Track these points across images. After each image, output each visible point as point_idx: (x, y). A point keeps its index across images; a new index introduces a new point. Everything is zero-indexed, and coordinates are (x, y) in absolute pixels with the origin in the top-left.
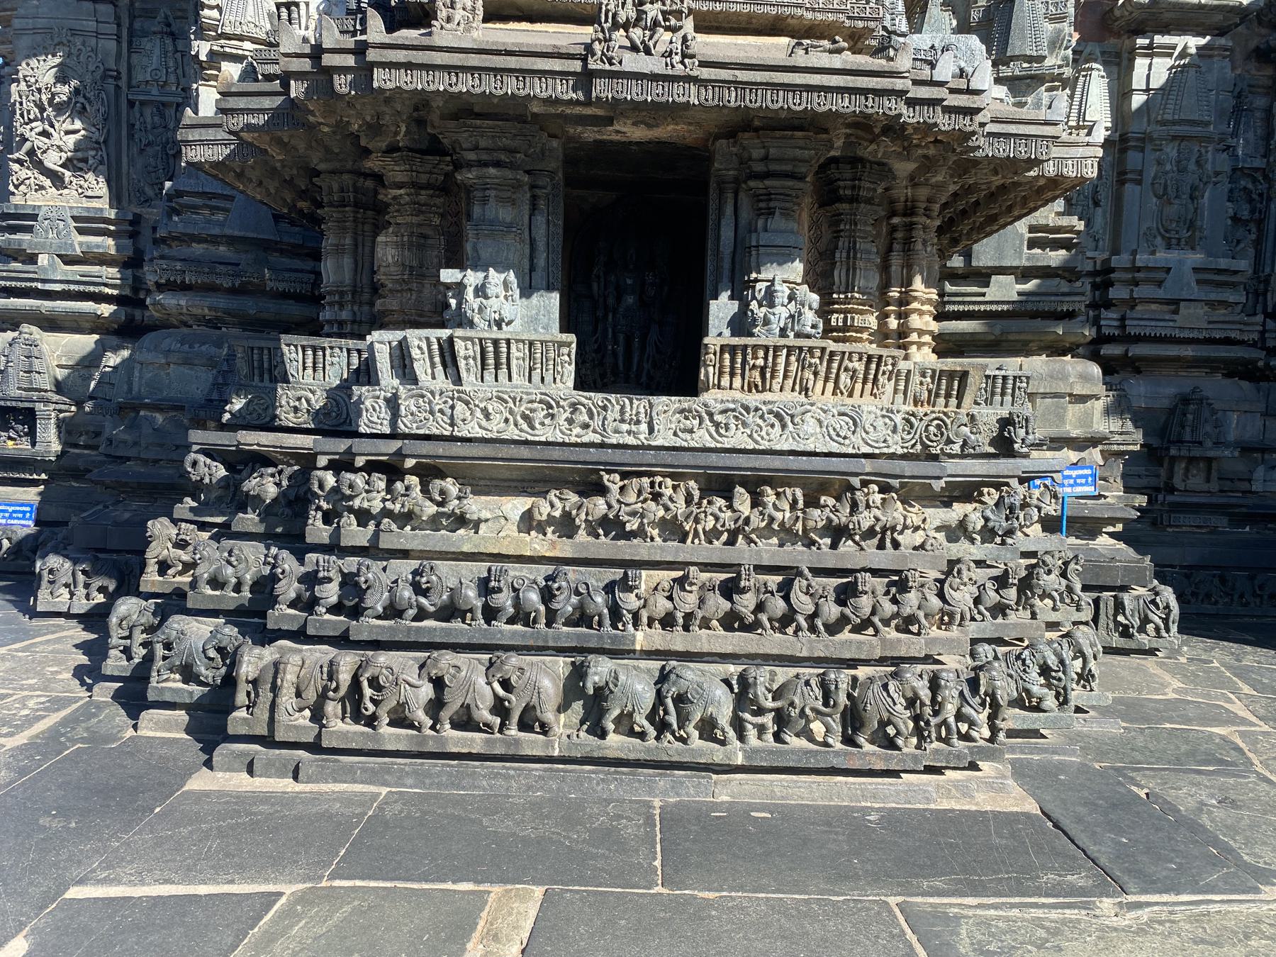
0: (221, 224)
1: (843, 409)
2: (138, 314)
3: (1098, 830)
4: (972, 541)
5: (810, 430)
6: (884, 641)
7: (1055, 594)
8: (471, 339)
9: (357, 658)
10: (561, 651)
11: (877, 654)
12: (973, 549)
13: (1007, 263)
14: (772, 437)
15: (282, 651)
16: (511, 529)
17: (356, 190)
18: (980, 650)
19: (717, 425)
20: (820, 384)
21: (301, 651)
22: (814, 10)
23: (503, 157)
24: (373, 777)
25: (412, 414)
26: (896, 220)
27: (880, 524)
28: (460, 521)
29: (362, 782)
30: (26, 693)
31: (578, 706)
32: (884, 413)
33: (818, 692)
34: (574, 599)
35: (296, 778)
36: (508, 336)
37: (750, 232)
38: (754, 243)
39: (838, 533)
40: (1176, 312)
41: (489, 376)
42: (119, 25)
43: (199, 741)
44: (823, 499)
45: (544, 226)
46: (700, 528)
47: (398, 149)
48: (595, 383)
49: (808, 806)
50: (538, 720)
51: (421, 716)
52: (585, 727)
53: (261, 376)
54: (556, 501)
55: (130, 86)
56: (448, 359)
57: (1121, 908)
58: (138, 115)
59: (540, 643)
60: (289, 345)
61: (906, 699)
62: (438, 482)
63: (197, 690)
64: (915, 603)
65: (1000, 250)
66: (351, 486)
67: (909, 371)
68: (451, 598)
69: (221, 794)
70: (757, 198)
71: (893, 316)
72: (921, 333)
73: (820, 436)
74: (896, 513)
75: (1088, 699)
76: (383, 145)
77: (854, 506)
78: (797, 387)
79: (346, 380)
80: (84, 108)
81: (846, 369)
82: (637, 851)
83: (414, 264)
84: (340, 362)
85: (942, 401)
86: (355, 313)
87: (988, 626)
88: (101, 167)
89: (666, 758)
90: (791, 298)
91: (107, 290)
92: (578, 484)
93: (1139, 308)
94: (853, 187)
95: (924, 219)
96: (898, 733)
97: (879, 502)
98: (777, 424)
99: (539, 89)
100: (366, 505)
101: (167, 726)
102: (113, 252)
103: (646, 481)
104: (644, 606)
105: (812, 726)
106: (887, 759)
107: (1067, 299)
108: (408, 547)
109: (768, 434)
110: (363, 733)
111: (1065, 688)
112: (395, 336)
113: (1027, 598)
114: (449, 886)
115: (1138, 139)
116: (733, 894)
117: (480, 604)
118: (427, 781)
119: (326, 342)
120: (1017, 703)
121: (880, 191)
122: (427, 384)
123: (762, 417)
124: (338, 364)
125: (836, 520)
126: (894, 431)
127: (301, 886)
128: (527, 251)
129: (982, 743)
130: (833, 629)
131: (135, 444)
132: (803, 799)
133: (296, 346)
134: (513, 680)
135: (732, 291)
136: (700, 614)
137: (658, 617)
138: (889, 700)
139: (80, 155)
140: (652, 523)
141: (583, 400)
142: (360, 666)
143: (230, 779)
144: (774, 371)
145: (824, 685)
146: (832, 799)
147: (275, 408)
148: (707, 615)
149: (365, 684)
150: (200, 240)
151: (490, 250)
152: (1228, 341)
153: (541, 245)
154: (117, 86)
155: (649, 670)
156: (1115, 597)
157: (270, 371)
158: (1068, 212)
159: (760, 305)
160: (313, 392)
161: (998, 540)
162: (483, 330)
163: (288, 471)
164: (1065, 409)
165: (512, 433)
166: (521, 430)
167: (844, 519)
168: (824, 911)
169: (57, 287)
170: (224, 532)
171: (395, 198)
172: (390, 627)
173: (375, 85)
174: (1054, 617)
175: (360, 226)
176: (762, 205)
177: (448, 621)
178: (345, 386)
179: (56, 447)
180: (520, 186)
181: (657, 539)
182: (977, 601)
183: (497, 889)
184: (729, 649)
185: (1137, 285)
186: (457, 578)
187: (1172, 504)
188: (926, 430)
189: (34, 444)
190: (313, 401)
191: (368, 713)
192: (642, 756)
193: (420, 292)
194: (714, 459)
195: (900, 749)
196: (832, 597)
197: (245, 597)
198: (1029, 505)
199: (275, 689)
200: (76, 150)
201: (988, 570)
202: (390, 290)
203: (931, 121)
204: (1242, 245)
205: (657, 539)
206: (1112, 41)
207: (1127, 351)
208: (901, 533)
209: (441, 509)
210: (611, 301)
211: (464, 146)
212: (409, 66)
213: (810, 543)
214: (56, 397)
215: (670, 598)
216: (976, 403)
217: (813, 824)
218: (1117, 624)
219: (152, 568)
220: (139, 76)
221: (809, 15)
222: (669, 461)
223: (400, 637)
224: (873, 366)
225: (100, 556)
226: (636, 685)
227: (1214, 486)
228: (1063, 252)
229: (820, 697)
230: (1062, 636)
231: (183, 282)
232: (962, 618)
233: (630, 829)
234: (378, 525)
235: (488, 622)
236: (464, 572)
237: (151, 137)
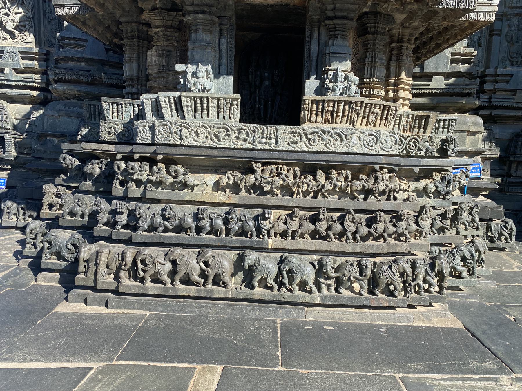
0: (82, 53)
1: (371, 132)
2: (49, 96)
3: (494, 338)
4: (429, 197)
5: (355, 142)
6: (389, 245)
7: (466, 223)
8: (189, 97)
9: (136, 250)
10: (232, 248)
11: (386, 251)
12: (430, 201)
13: (440, 70)
14: (336, 145)
15: (101, 246)
16: (209, 190)
18: (433, 249)
21: (109, 246)
23: (206, 9)
24: (143, 307)
25: (161, 134)
26: (393, 45)
27: (388, 188)
28: (185, 185)
29: (138, 309)
31: (241, 274)
32: (391, 134)
34: (239, 224)
35: (107, 306)
36: (208, 95)
37: (326, 46)
38: (327, 52)
39: (367, 193)
40: (515, 95)
41: (198, 115)
43: (64, 287)
44: (361, 176)
45: (226, 44)
46: (300, 190)
47: (157, 9)
49: (351, 323)
50: (221, 280)
51: (166, 278)
52: (244, 284)
53: (95, 118)
56: (179, 107)
57: (513, 381)
58: (47, 6)
59: (223, 244)
60: (105, 102)
63: (64, 264)
64: (404, 226)
65: (437, 64)
66: (132, 169)
68: (180, 222)
69: (70, 314)
70: (329, 30)
71: (391, 91)
72: (404, 99)
73: (360, 145)
74: (396, 183)
75: (481, 271)
76: (150, 7)
77: (376, 179)
78: (349, 121)
79: (132, 119)
81: (373, 113)
82: (269, 346)
83: (165, 64)
84: (128, 111)
85: (416, 130)
86: (138, 90)
87: (438, 238)
88: (31, 29)
90: (346, 78)
91: (35, 85)
93: (497, 93)
94: (375, 27)
95: (407, 44)
96: (396, 289)
97: (388, 178)
98: (339, 139)
100: (139, 177)
101: (50, 280)
102: (37, 67)
103: (274, 167)
104: (273, 227)
105: (353, 285)
106: (390, 301)
107: (468, 87)
108: (160, 198)
109: (334, 144)
110: (138, 286)
111: (473, 268)
112: (153, 96)
113: (455, 225)
114: (176, 365)
116: (317, 371)
117: (194, 225)
119: (122, 101)
120: (451, 275)
123: (331, 136)
124: (128, 111)
125: (367, 187)
126: (396, 143)
127: (102, 364)
128: (218, 56)
129: (435, 294)
130: (364, 239)
131: (45, 152)
133: (108, 103)
135: (317, 76)
136: (300, 231)
137: (279, 232)
138: (392, 273)
139: (22, 24)
140: (277, 187)
141: (244, 127)
142: (137, 254)
143: (76, 306)
145: (360, 266)
146: (362, 320)
147: (100, 132)
148: (303, 232)
149: (139, 263)
150: (73, 60)
151: (199, 55)
153: (224, 53)
155: (275, 258)
156: (487, 224)
157: (99, 116)
158: (469, 46)
159: (331, 82)
160: (117, 125)
161: (441, 197)
162: (195, 93)
163: (105, 161)
164: (465, 138)
165: (209, 143)
166: (214, 142)
167: (371, 186)
168: (363, 381)
169: (13, 83)
170: (77, 191)
171: (156, 33)
172: (151, 236)
174: (465, 233)
176: (332, 33)
177: (178, 232)
178: (131, 122)
179: (14, 154)
180: (214, 24)
181: (279, 195)
182: (432, 225)
183: (199, 367)
184: (314, 248)
185: (497, 83)
186: (183, 213)
187: (509, 182)
188: (409, 144)
189: (4, 153)
190: (117, 129)
192: (271, 298)
193: (168, 78)
194: (308, 156)
195: (396, 297)
196: (364, 224)
197: (85, 221)
199: (97, 264)
200: (20, 22)
201: (437, 211)
202: (154, 77)
205: (279, 195)
207: (491, 113)
208: (398, 193)
209: (175, 180)
210: (258, 84)
211: (187, 3)
213: (354, 198)
214: (13, 132)
215: (285, 223)
217: (354, 333)
218: (488, 236)
219: (45, 207)
223: (156, 241)
224: (386, 111)
225: (30, 201)
226: (269, 265)
228: (467, 65)
229: (358, 272)
230: (469, 242)
231: (65, 79)
233: (265, 335)
234: (145, 187)
235: (198, 234)
236: (186, 210)
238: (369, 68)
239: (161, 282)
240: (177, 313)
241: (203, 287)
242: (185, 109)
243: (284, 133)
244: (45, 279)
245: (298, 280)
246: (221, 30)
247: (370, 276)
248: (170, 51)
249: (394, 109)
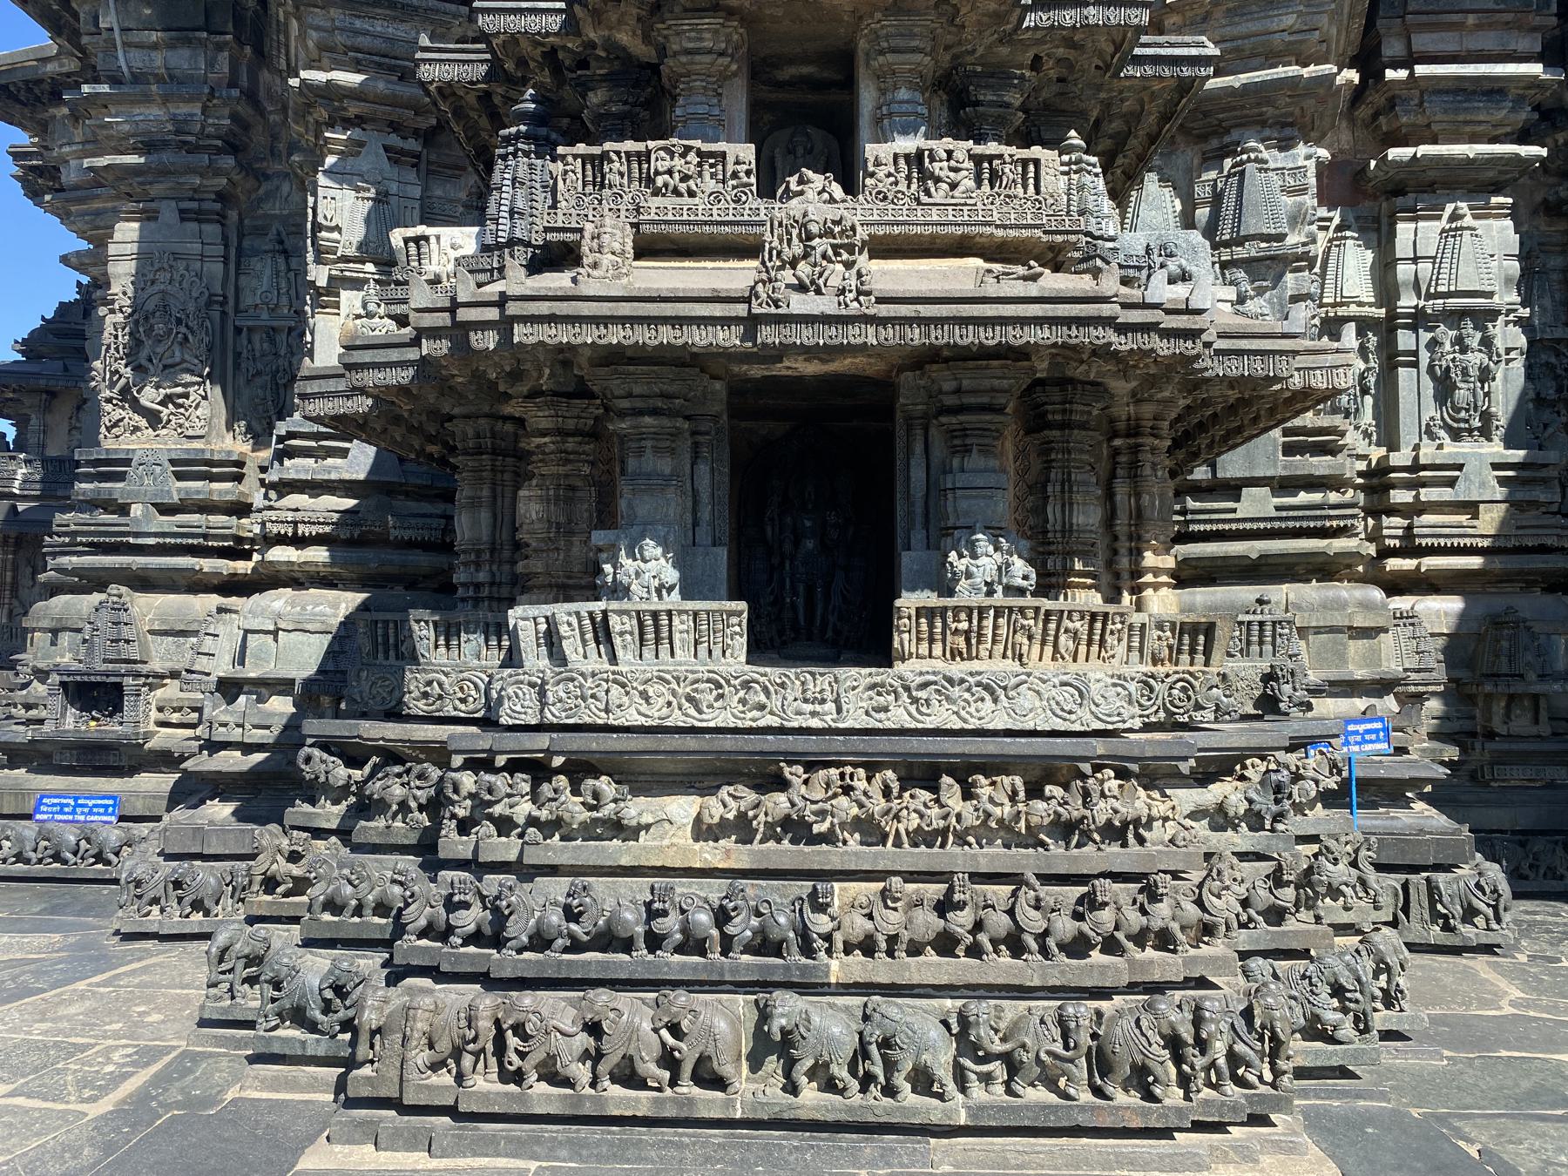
1: (1065, 678)
10: (740, 987)
11: (1125, 980)
13: (1259, 473)
15: (410, 991)
17: (494, 436)
19: (915, 701)
20: (1036, 648)
22: (1005, 227)
24: (519, 1149)
26: (1117, 442)
28: (618, 828)
29: (507, 1156)
30: (110, 1042)
33: (1056, 1032)
34: (755, 922)
36: (670, 607)
37: (945, 473)
38: (949, 486)
40: (1475, 516)
41: (648, 653)
42: (226, 246)
44: (1048, 788)
45: (708, 476)
46: (902, 828)
47: (541, 393)
48: (771, 640)
54: (728, 799)
55: (237, 311)
59: (715, 978)
60: (418, 621)
61: (1163, 1037)
62: (590, 782)
66: (490, 792)
67: (1144, 625)
68: (608, 922)
70: (951, 433)
72: (1156, 572)
74: (1141, 802)
75: (1400, 1020)
77: (1086, 794)
78: (1009, 653)
80: (186, 339)
81: (1067, 631)
83: (562, 520)
85: (1185, 658)
86: (493, 575)
87: (1263, 934)
89: (871, 1119)
92: (755, 776)
94: (1064, 411)
98: (988, 697)
99: (699, 337)
100: (507, 812)
103: (834, 772)
106: (1144, 1113)
110: (506, 1094)
115: (1407, 316)
118: (584, 1152)
121: (1095, 412)
122: (578, 666)
123: (969, 690)
128: (690, 504)
129: (1263, 1089)
132: (1043, 1167)
133: (427, 622)
134: (685, 1025)
136: (905, 936)
138: (1143, 1040)
143: (350, 1154)
144: (980, 635)
145: (1062, 1022)
146: (1078, 1168)
152: (1543, 549)
153: (705, 497)
154: (224, 313)
155: (847, 1008)
157: (396, 646)
160: (446, 674)
164: (1345, 646)
166: (687, 715)
169: (151, 541)
171: (538, 446)
173: (516, 339)
174: (1346, 918)
175: (499, 476)
176: (957, 442)
182: (1245, 903)
184: (944, 980)
190: (446, 686)
191: (511, 1068)
192: (843, 1117)
195: (1159, 1101)
198: (1302, 778)
202: (535, 551)
203: (1148, 347)
204: (1550, 430)
206: (1367, 203)
209: (595, 814)
210: (787, 547)
212: (552, 319)
215: (870, 917)
216: (1230, 655)
220: (248, 300)
221: (1000, 233)
222: (861, 748)
223: (550, 973)
224: (1099, 625)
227: (1545, 729)
232: (1228, 928)
235: (652, 950)
236: (622, 891)
237: (260, 366)
238: (1058, 508)
239: (567, 1082)
240: (607, 1162)
241: (668, 1092)
242: (617, 641)
243: (854, 688)
244: (262, 1082)
245: (908, 1066)
246: (696, 445)
247: (1090, 1048)
248: (573, 488)
249: (1118, 619)
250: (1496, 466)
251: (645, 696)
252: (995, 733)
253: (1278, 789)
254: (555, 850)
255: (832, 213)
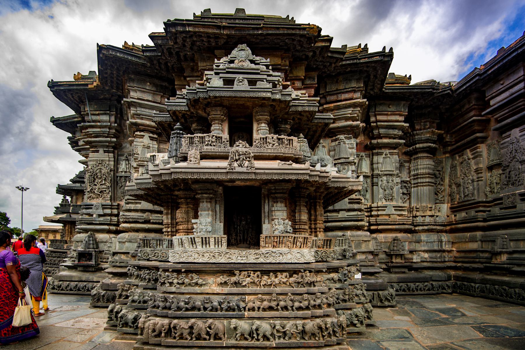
41: (204, 246)
85: (325, 247)
98: (281, 256)
103: (246, 273)
136: (262, 307)
246: (216, 201)
250: (394, 207)
251: (203, 255)
252: (283, 263)
253: (345, 274)
254: (183, 289)
255: (244, 150)
